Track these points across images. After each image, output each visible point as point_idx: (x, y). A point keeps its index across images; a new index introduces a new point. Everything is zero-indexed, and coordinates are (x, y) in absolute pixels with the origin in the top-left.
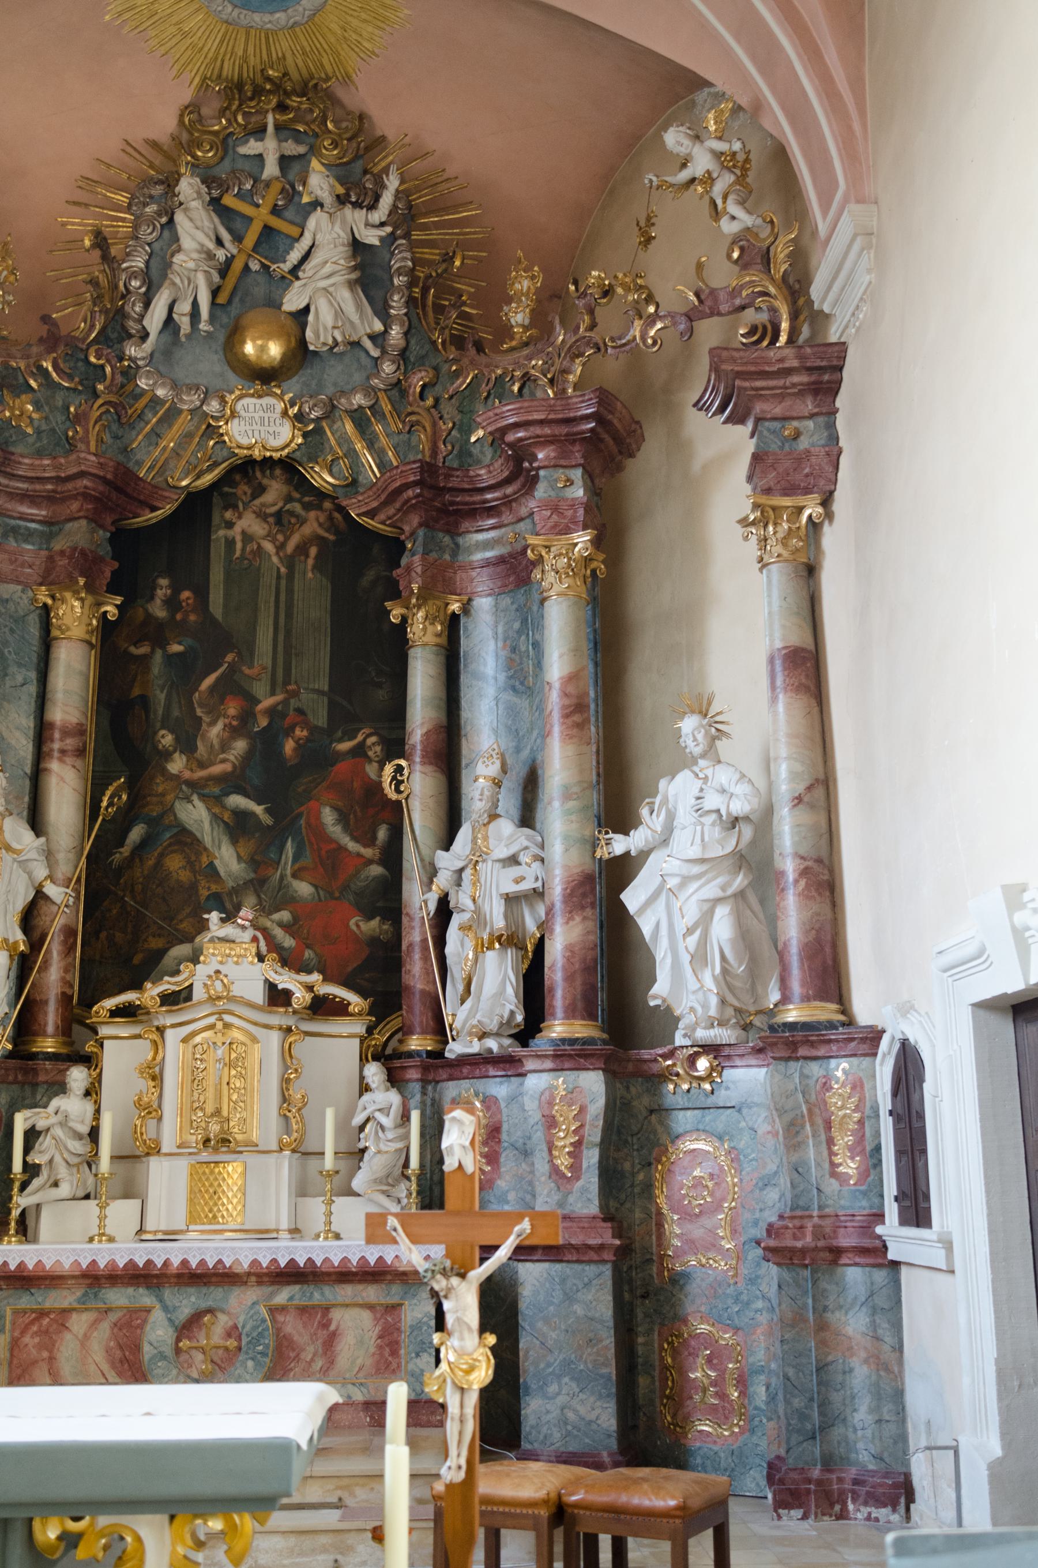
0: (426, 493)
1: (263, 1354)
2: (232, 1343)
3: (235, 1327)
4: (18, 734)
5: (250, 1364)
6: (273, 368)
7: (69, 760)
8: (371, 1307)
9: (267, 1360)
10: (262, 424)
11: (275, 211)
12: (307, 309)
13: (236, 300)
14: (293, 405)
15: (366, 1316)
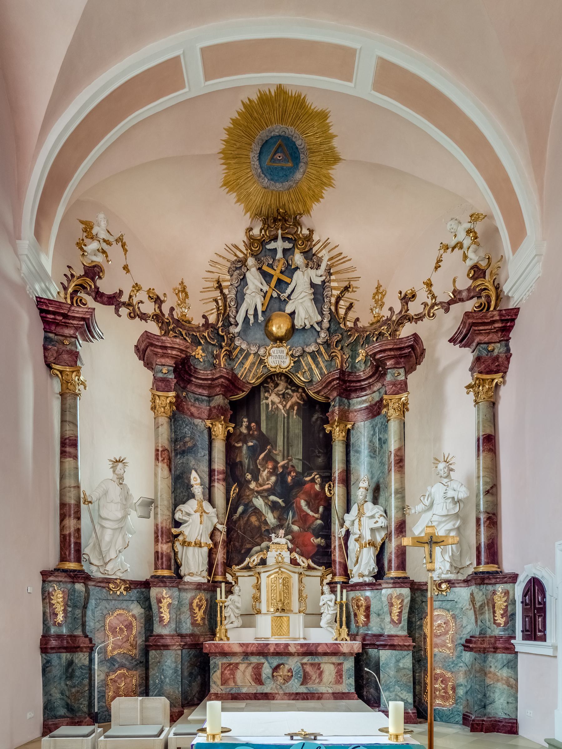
0: (341, 383)
1: (300, 677)
2: (290, 674)
3: (291, 669)
4: (203, 473)
5: (296, 680)
6: (282, 336)
7: (221, 482)
8: (334, 664)
9: (301, 679)
10: (280, 358)
11: (282, 272)
12: (293, 313)
13: (268, 309)
14: (290, 350)
15: (332, 667)
